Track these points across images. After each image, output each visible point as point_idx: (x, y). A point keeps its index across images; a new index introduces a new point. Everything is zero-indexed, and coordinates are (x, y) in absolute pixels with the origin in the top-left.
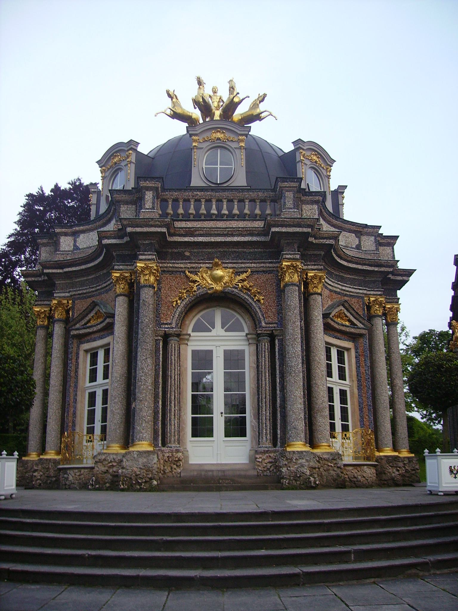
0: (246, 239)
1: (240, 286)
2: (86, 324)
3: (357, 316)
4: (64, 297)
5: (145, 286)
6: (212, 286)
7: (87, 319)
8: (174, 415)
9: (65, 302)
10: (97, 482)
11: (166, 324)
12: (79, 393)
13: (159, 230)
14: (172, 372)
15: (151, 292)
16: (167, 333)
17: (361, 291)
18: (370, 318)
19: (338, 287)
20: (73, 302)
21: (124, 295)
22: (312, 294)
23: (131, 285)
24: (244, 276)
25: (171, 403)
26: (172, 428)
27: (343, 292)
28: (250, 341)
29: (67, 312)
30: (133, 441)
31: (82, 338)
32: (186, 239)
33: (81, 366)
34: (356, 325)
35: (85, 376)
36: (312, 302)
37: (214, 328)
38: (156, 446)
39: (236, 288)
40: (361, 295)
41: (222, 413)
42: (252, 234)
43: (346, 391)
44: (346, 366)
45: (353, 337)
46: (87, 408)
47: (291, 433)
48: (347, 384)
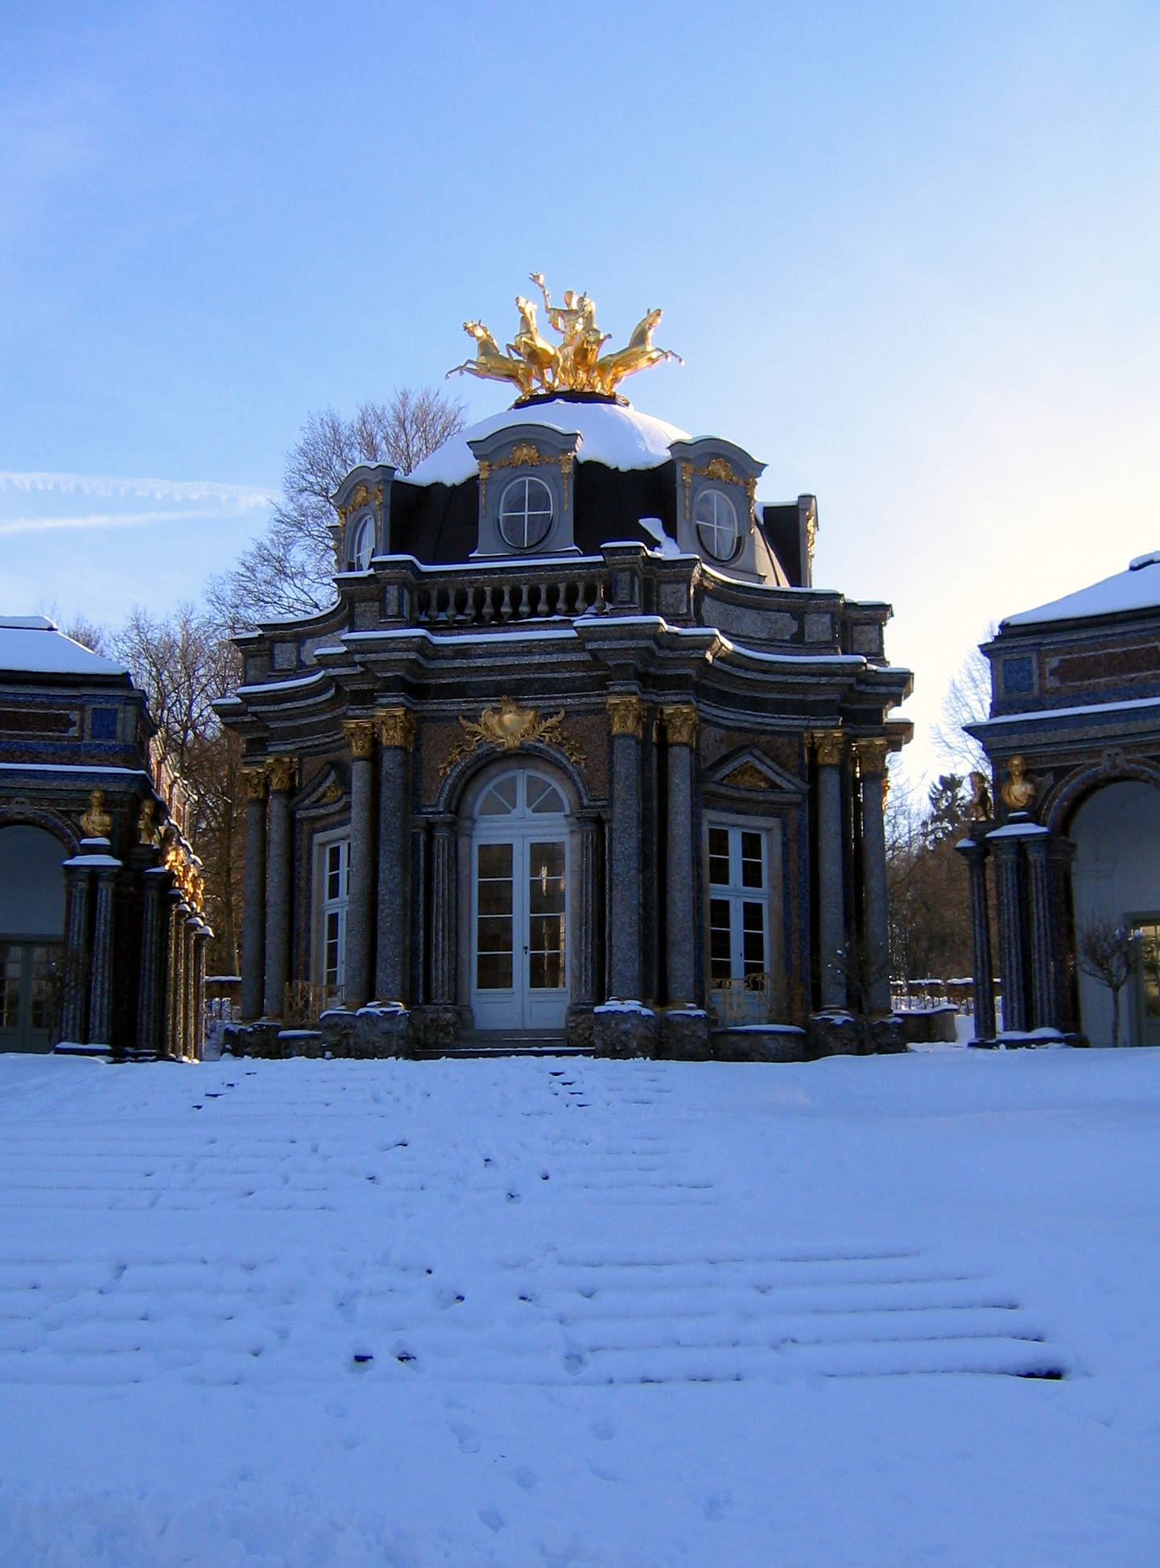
1: (547, 738)
2: (319, 800)
5: (389, 747)
6: (502, 740)
7: (321, 790)
8: (443, 953)
9: (287, 760)
11: (429, 806)
12: (314, 916)
13: (404, 655)
16: (432, 821)
17: (796, 722)
18: (813, 771)
19: (747, 719)
20: (300, 760)
21: (364, 759)
22: (672, 745)
24: (554, 720)
25: (437, 934)
27: (757, 727)
28: (573, 828)
29: (292, 777)
32: (457, 663)
34: (780, 788)
35: (321, 884)
36: (671, 760)
37: (514, 807)
39: (541, 742)
40: (796, 730)
41: (526, 948)
43: (761, 905)
45: (776, 810)
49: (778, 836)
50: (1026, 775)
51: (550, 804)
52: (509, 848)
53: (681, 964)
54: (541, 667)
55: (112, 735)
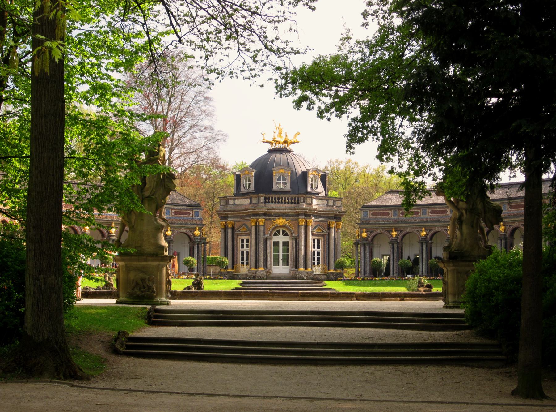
0: (290, 211)
3: (324, 229)
4: (231, 221)
10: (249, 278)
14: (268, 248)
15: (263, 227)
18: (329, 228)
23: (256, 223)
26: (268, 264)
30: (258, 267)
31: (238, 235)
32: (272, 211)
33: (238, 243)
38: (264, 268)
42: (291, 210)
44: (320, 244)
45: (323, 236)
46: (241, 256)
47: (300, 266)
48: (320, 250)
49: (323, 240)
50: (366, 232)
51: (286, 234)
52: (278, 242)
53: (310, 263)
54: (287, 212)
55: (198, 216)
